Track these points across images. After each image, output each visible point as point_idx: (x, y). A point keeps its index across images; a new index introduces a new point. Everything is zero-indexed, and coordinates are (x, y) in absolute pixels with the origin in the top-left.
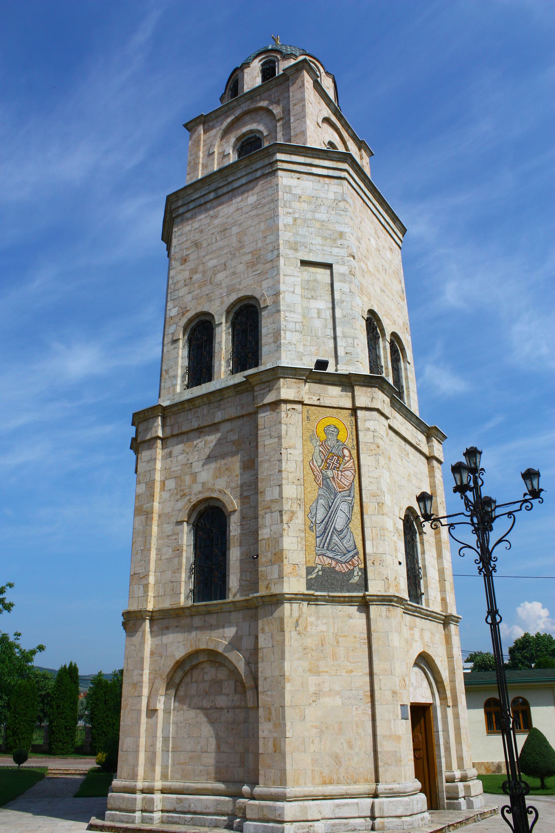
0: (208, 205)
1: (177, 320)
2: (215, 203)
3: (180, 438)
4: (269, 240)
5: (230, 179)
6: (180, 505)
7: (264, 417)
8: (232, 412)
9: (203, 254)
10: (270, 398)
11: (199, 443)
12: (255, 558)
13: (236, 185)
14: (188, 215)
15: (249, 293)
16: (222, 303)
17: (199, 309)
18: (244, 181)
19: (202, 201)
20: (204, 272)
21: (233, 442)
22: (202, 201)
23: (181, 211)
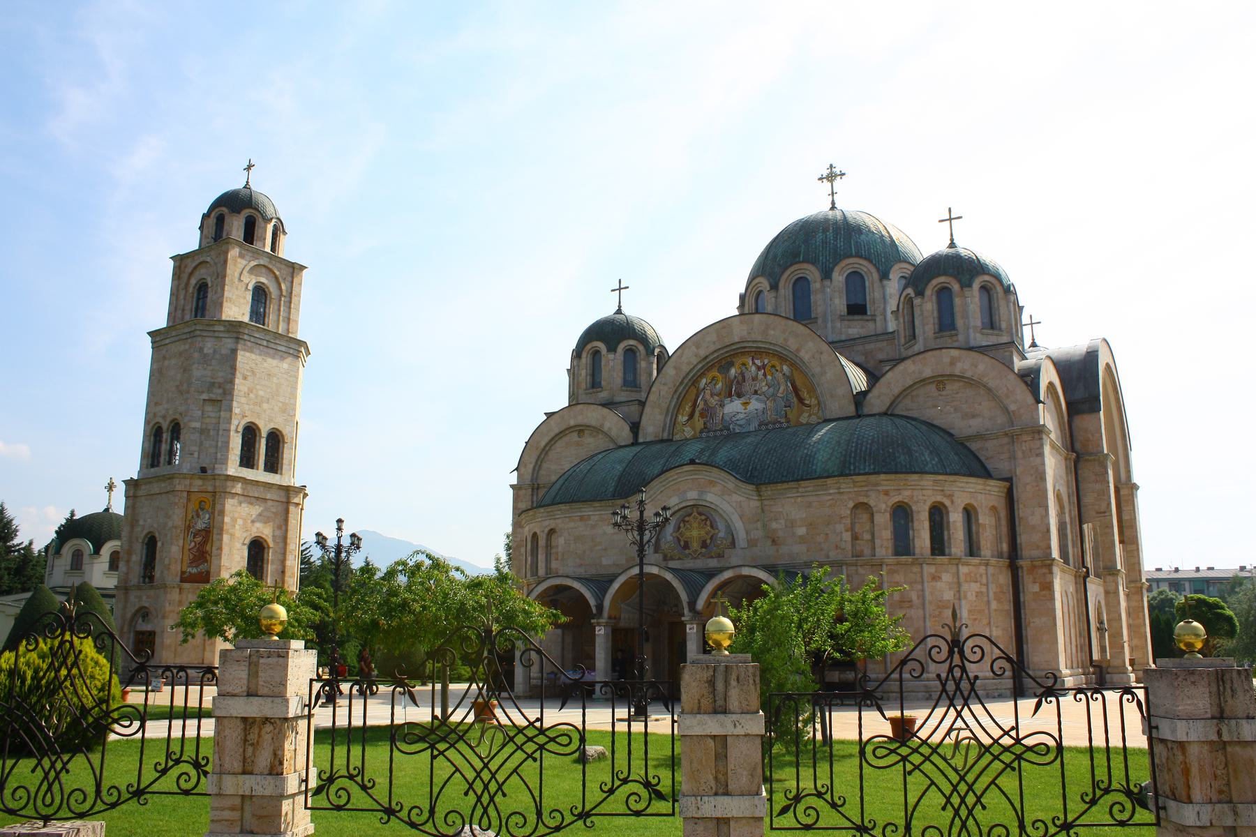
0: (261, 347)
1: (239, 417)
2: (265, 350)
3: (246, 498)
4: (292, 401)
5: (277, 342)
6: (245, 535)
7: (292, 508)
8: (275, 497)
9: (256, 382)
10: (296, 500)
11: (257, 507)
12: (283, 572)
13: (280, 348)
14: (249, 344)
15: (280, 429)
16: (266, 425)
17: (253, 421)
18: (283, 349)
19: (259, 342)
20: (257, 396)
21: (273, 513)
22: (259, 342)
23: (246, 337)
